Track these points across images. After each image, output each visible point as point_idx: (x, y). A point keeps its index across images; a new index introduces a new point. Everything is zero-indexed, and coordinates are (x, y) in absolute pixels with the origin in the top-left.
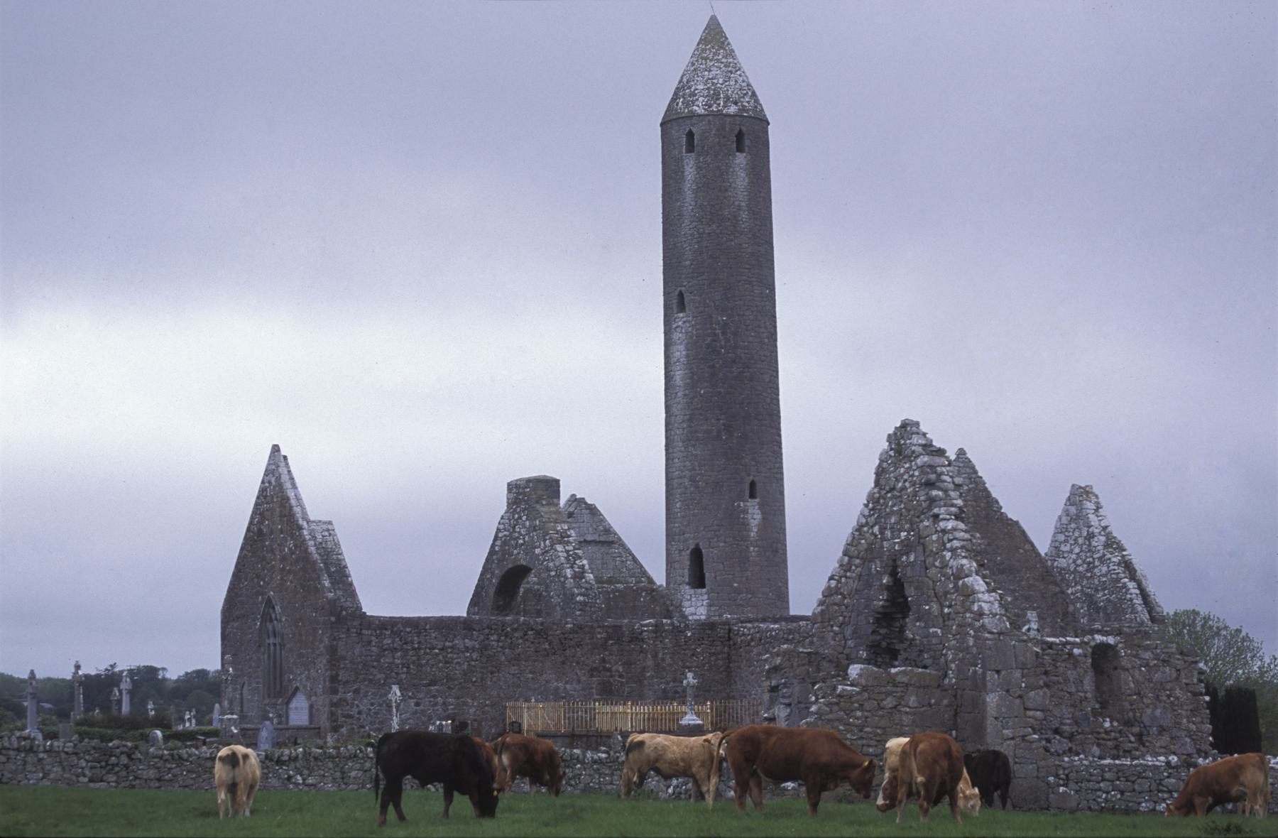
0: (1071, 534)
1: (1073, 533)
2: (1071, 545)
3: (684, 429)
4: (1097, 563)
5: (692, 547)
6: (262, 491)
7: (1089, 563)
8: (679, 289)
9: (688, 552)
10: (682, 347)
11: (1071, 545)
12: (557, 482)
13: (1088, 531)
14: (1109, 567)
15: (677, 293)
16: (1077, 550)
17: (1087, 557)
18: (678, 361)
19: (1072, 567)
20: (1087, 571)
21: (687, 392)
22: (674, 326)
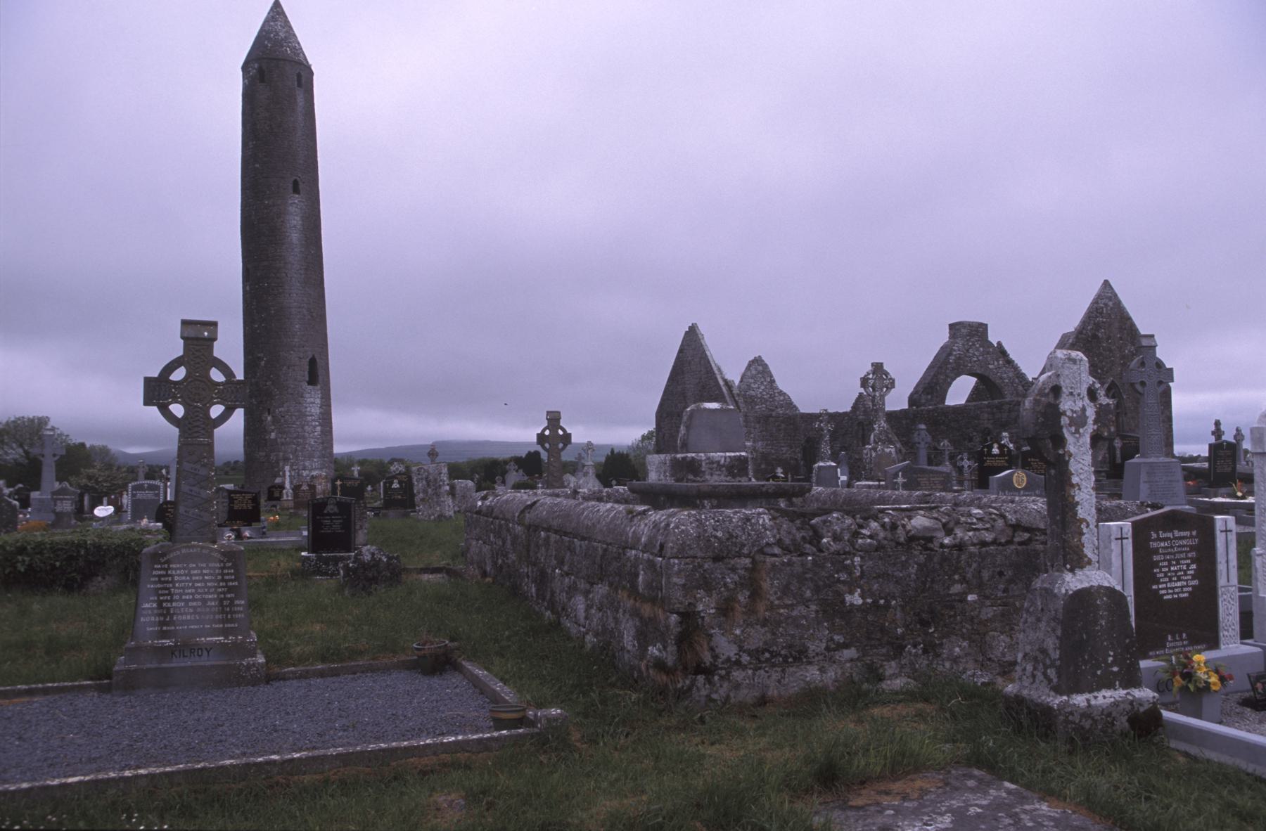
3: (301, 274)
5: (310, 357)
6: (1095, 302)
8: (295, 178)
9: (308, 360)
10: (298, 218)
12: (986, 325)
15: (292, 179)
16: (763, 387)
18: (295, 226)
19: (759, 396)
20: (770, 398)
21: (303, 250)
22: (290, 202)
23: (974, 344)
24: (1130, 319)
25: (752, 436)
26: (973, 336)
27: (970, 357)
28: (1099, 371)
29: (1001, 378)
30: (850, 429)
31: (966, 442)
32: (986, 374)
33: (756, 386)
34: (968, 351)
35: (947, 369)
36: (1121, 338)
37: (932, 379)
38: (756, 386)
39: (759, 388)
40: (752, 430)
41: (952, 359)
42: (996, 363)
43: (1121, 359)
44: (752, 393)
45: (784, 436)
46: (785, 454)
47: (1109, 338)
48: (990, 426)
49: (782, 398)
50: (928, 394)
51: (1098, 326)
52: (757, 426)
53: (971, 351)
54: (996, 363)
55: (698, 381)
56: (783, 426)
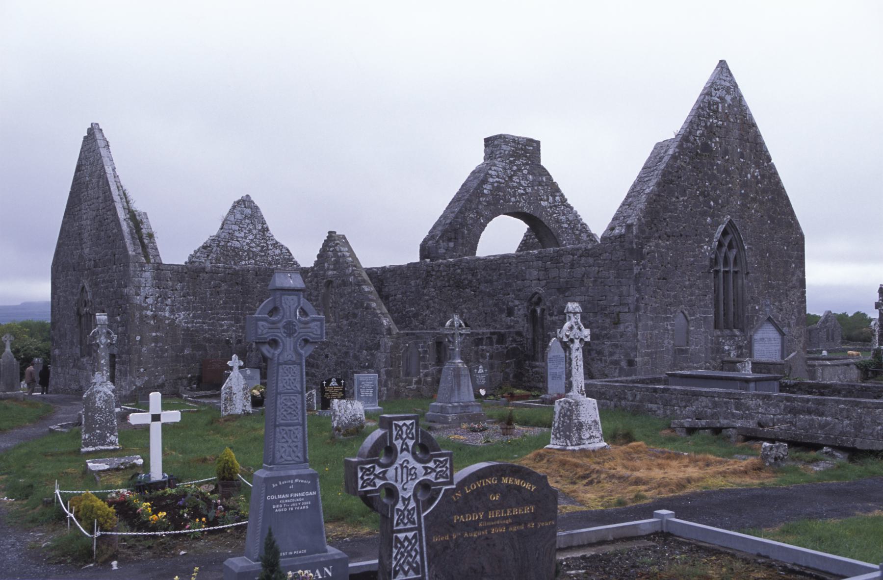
0: (246, 226)
1: (247, 226)
2: (245, 233)
4: (270, 247)
6: (707, 93)
7: (263, 247)
11: (245, 233)
13: (262, 227)
14: (281, 251)
16: (251, 237)
17: (261, 243)
19: (246, 248)
20: (261, 251)
23: (519, 170)
24: (754, 125)
25: (169, 301)
26: (518, 157)
27: (513, 187)
28: (712, 203)
29: (558, 221)
30: (315, 293)
31: (504, 316)
32: (537, 215)
33: (242, 234)
34: (511, 178)
35: (480, 202)
36: (742, 155)
37: (456, 217)
38: (242, 234)
39: (246, 238)
40: (170, 293)
41: (486, 190)
42: (551, 198)
43: (742, 188)
44: (237, 244)
45: (225, 303)
46: (227, 331)
47: (726, 152)
48: (541, 291)
49: (278, 252)
50: (450, 240)
51: (711, 131)
52: (179, 286)
53: (515, 179)
54: (551, 198)
55: (94, 213)
56: (224, 287)
